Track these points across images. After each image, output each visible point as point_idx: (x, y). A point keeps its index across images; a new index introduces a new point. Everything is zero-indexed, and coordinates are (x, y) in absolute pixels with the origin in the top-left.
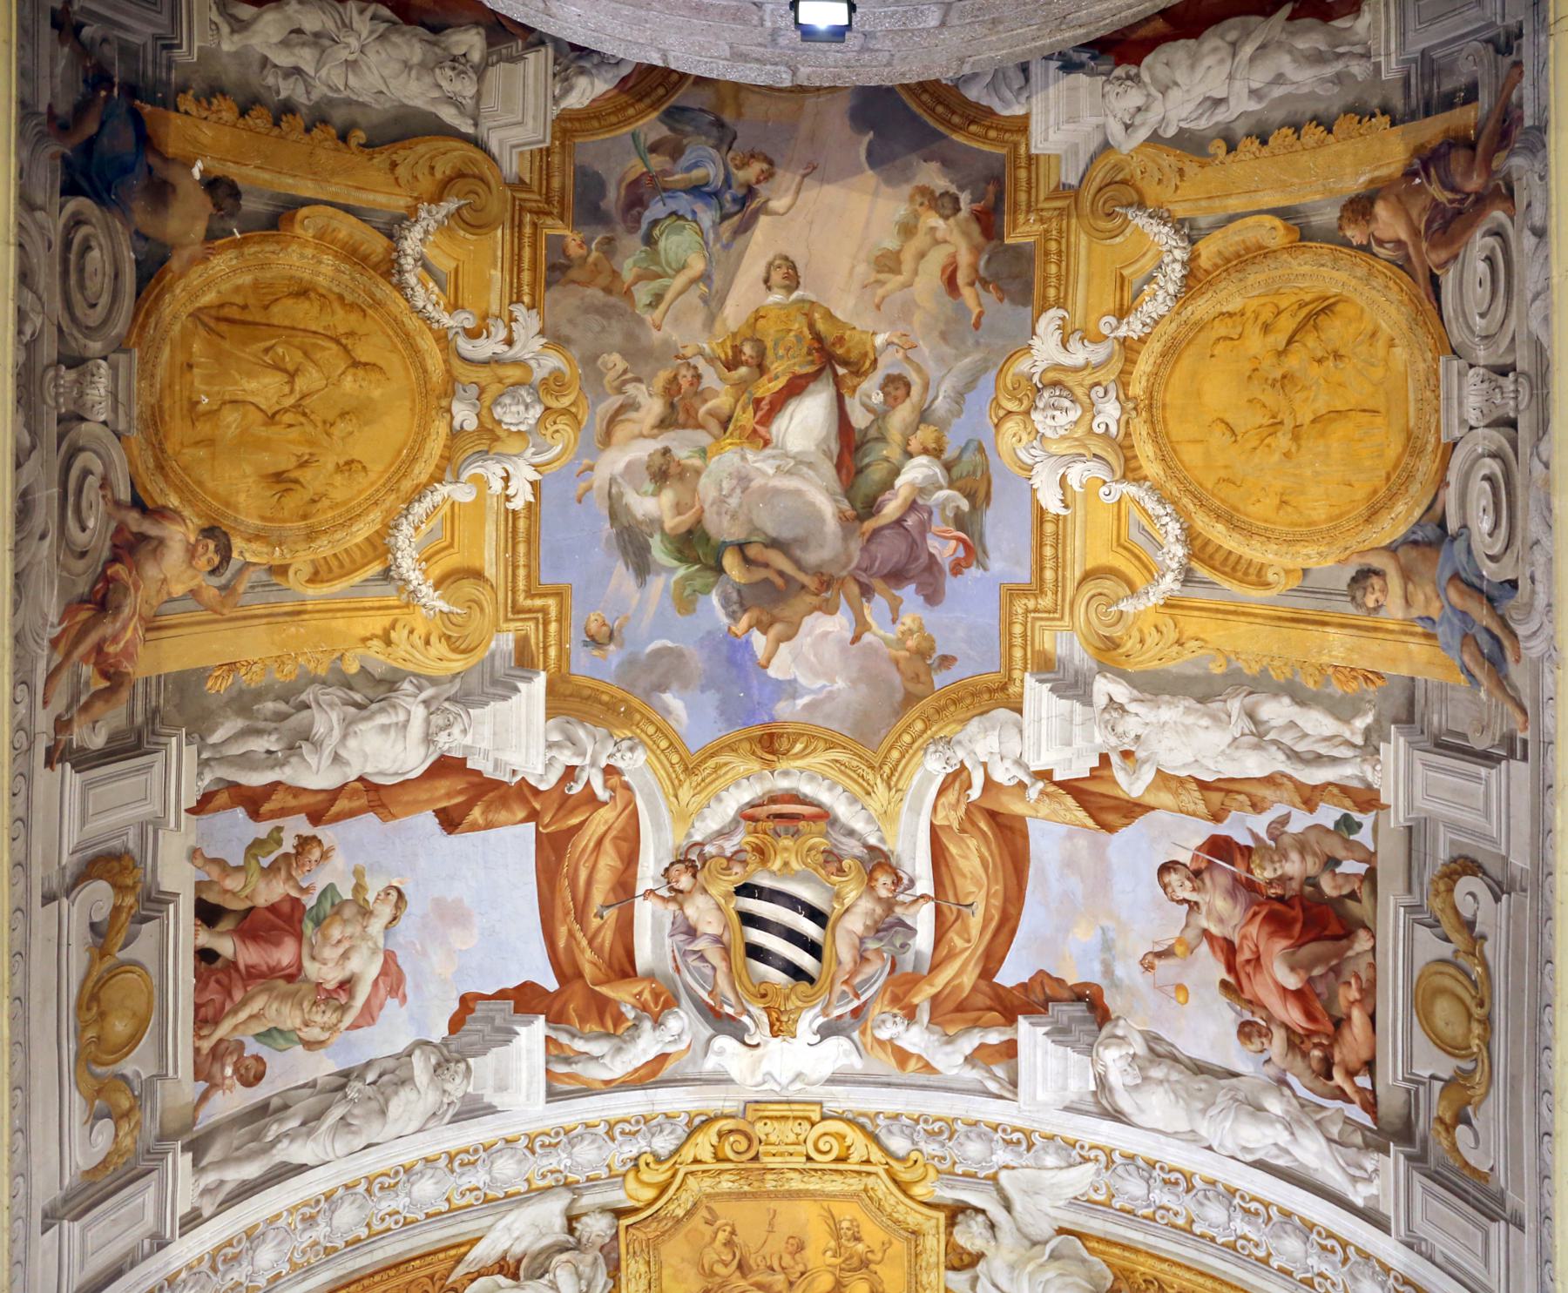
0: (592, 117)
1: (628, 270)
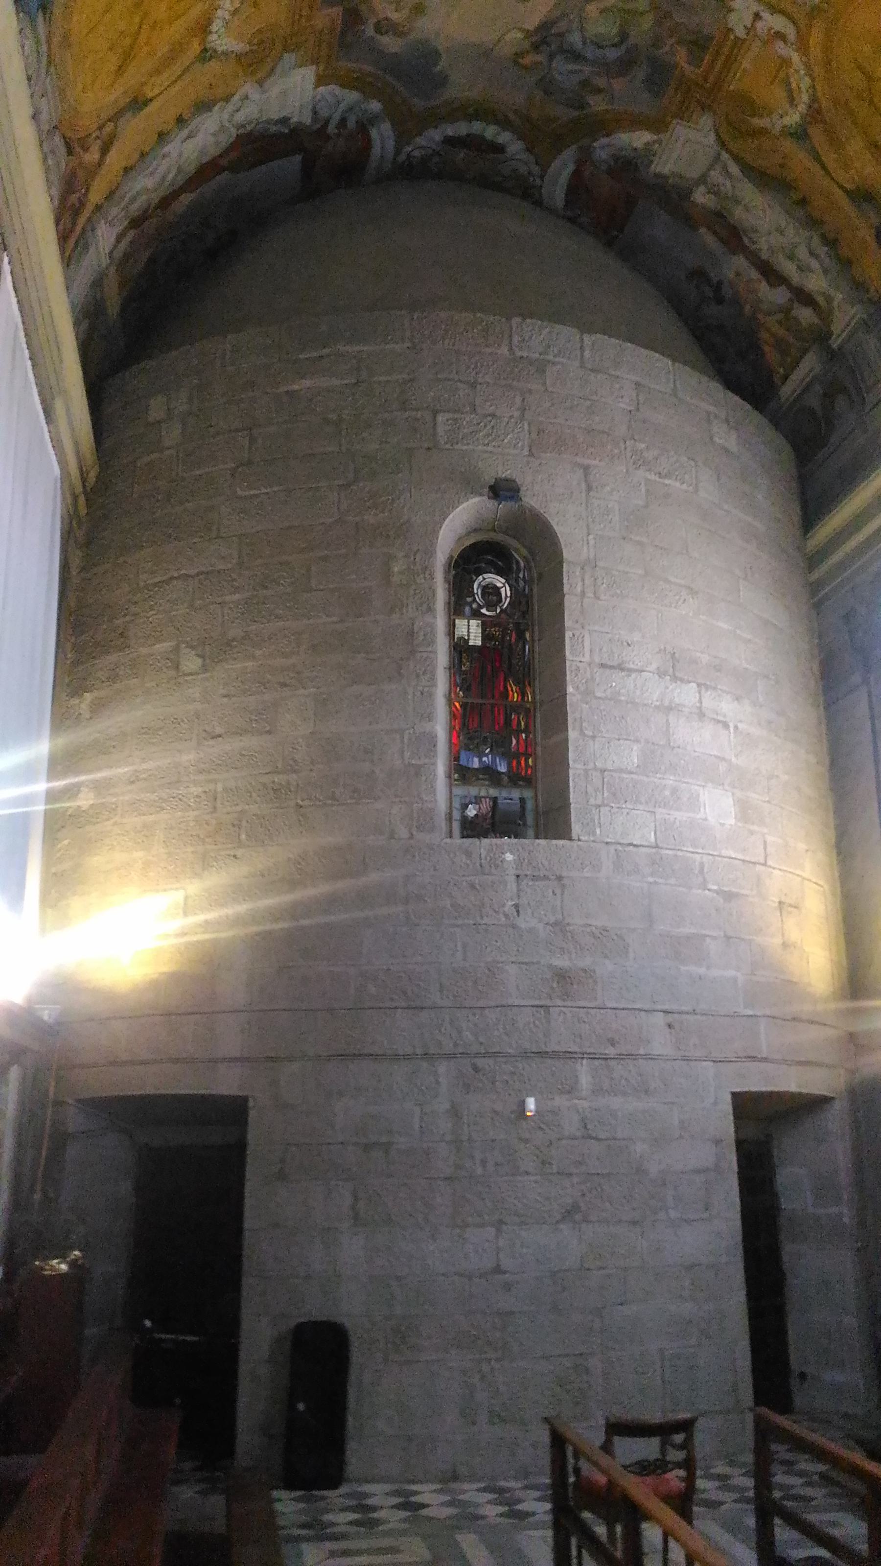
0: (636, 123)
1: (647, 23)
